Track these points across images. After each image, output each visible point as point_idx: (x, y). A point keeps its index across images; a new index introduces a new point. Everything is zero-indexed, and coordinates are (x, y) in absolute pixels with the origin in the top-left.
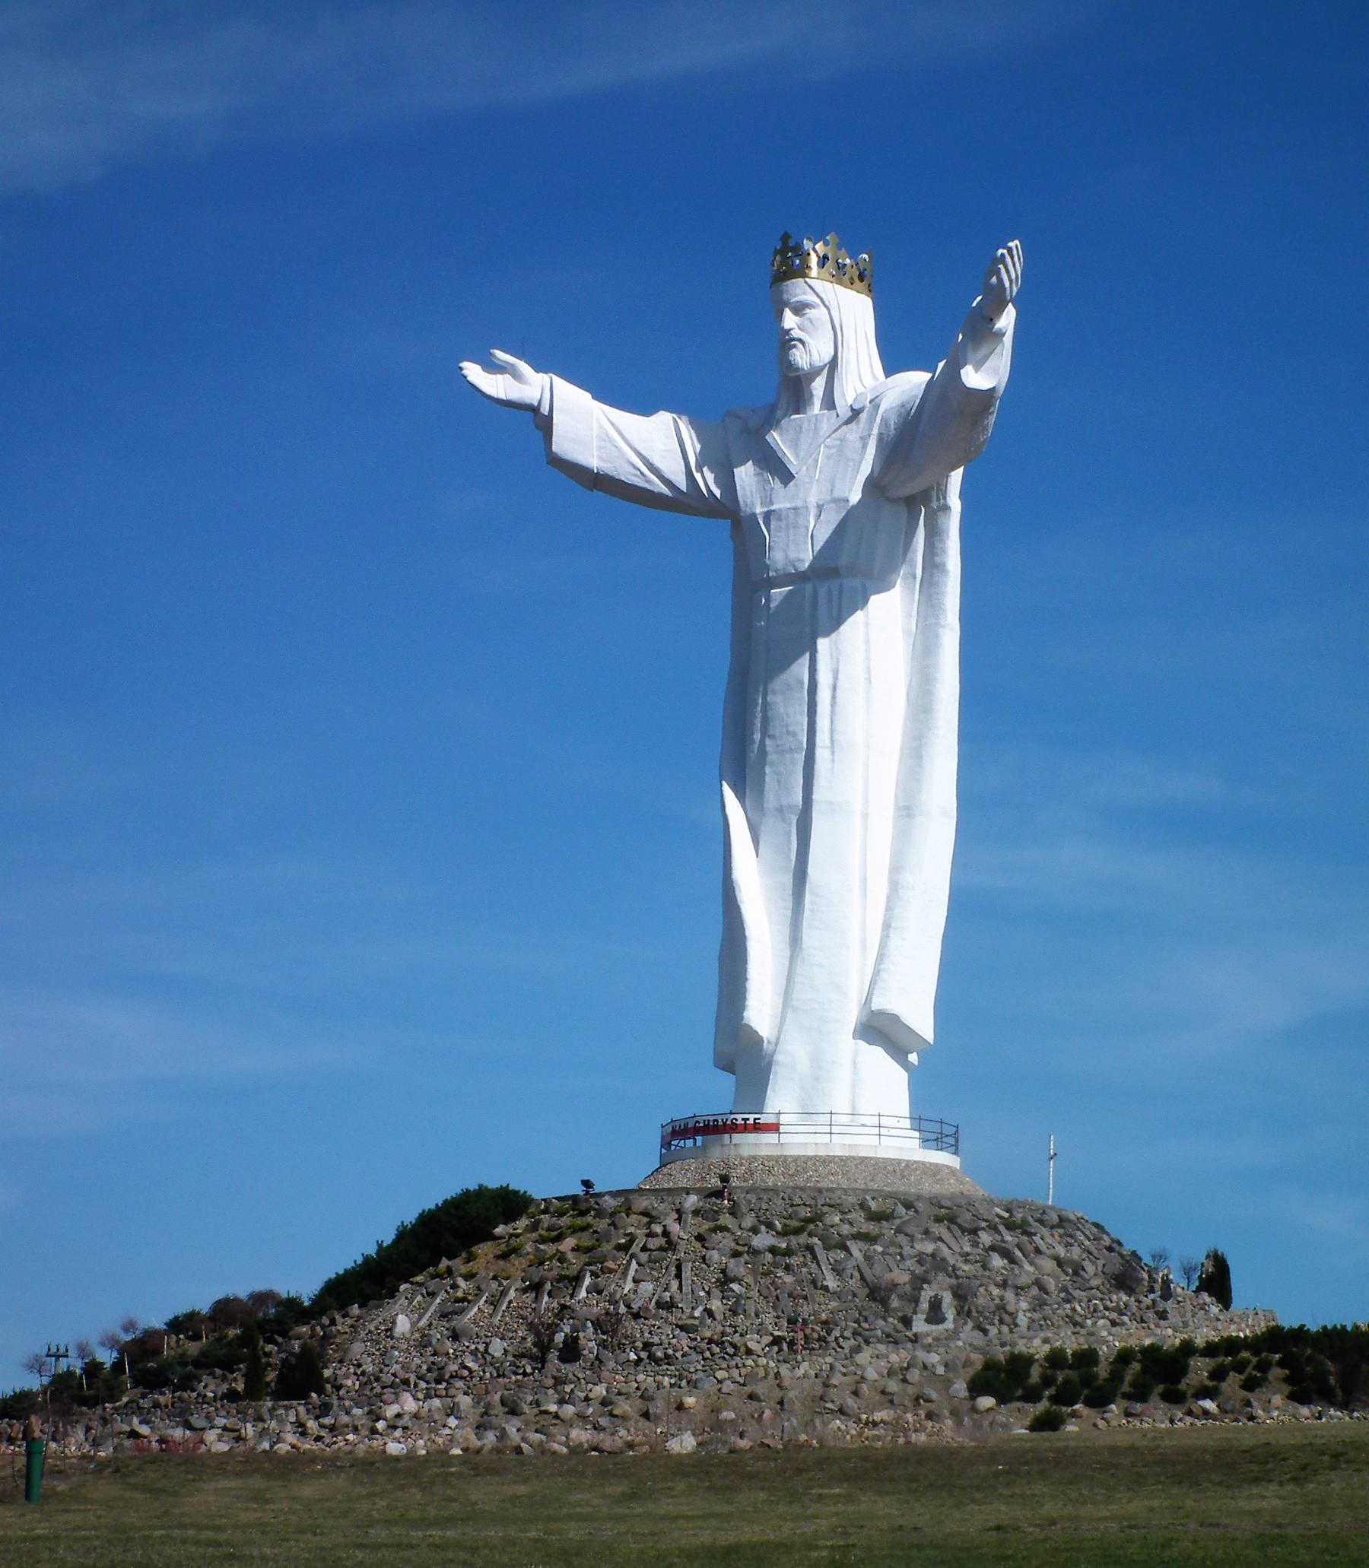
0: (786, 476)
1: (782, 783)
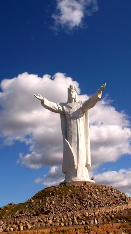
0: (71, 108)
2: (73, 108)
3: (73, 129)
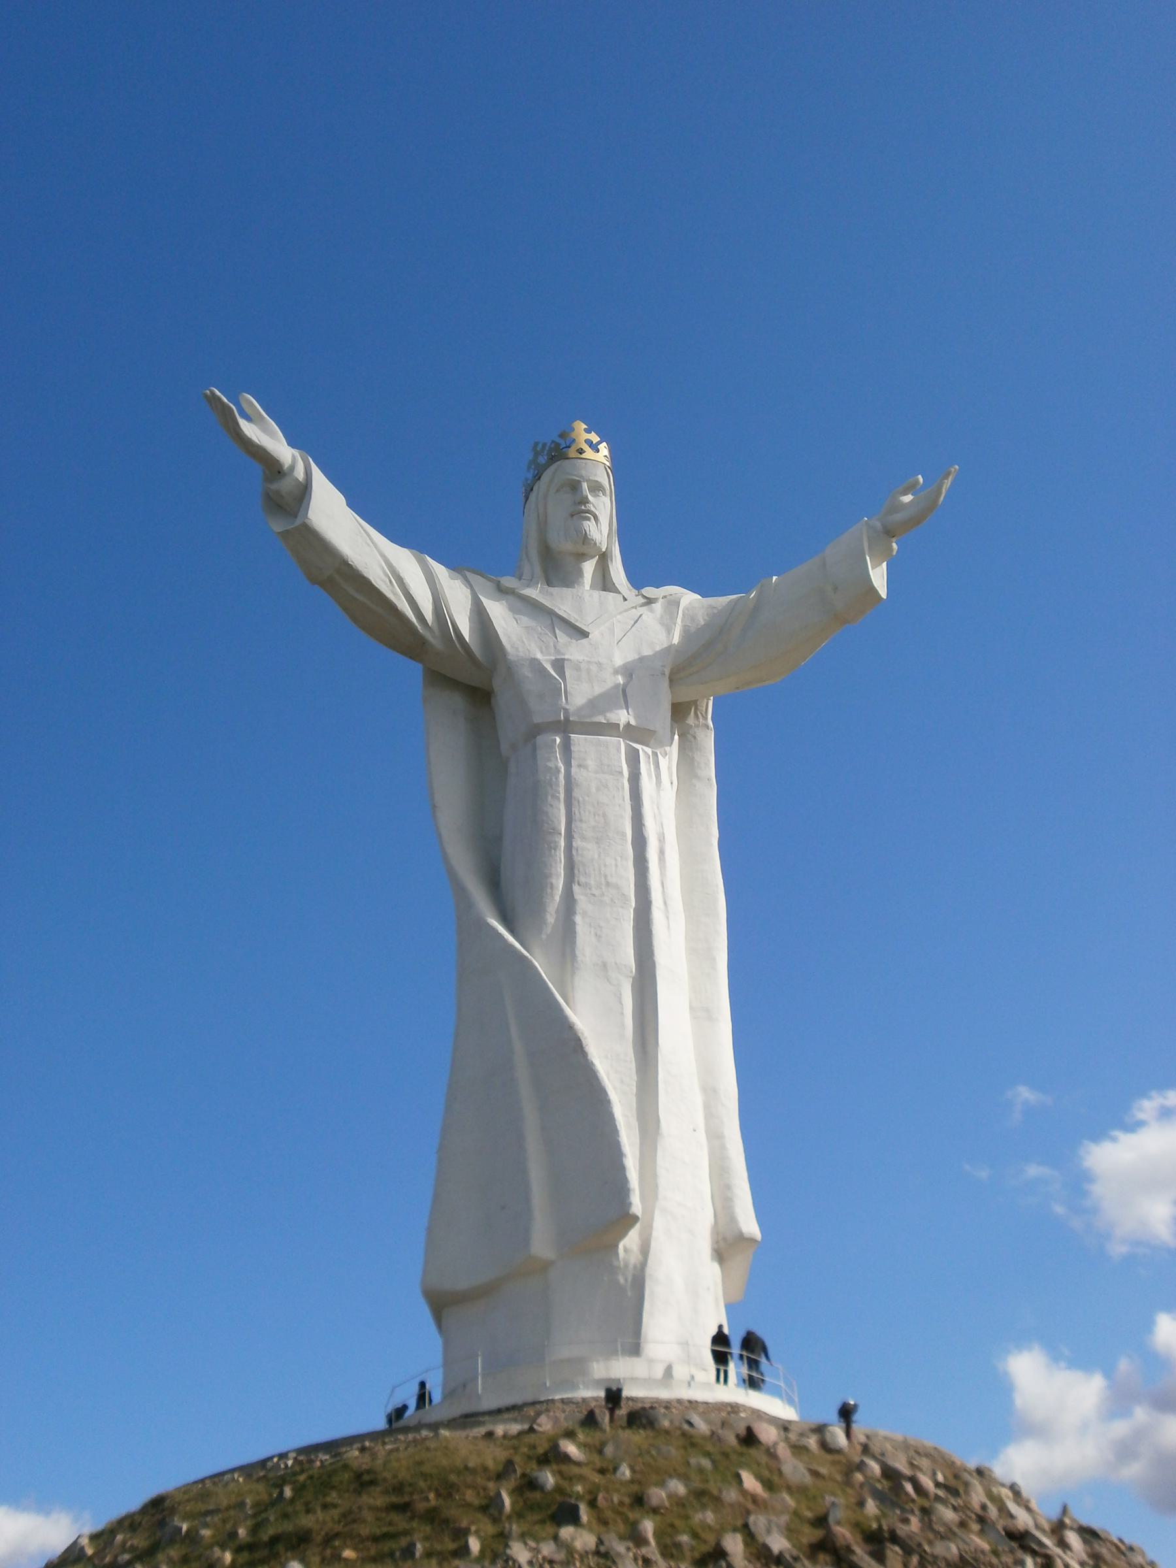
2: (595, 634)
3: (598, 841)
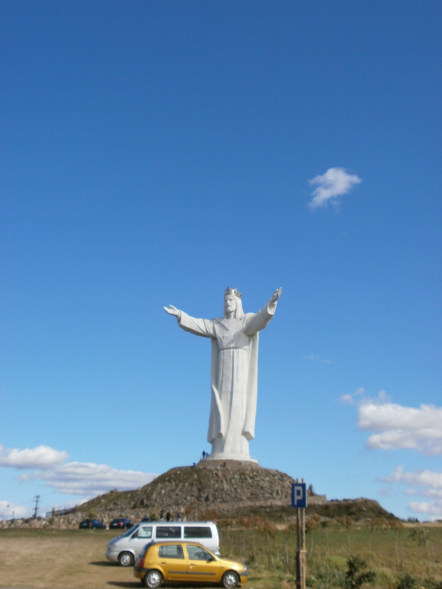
1: (227, 386)
